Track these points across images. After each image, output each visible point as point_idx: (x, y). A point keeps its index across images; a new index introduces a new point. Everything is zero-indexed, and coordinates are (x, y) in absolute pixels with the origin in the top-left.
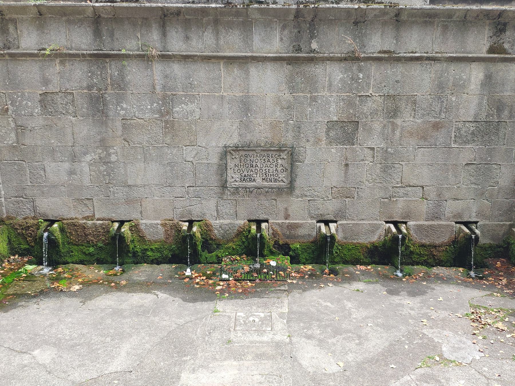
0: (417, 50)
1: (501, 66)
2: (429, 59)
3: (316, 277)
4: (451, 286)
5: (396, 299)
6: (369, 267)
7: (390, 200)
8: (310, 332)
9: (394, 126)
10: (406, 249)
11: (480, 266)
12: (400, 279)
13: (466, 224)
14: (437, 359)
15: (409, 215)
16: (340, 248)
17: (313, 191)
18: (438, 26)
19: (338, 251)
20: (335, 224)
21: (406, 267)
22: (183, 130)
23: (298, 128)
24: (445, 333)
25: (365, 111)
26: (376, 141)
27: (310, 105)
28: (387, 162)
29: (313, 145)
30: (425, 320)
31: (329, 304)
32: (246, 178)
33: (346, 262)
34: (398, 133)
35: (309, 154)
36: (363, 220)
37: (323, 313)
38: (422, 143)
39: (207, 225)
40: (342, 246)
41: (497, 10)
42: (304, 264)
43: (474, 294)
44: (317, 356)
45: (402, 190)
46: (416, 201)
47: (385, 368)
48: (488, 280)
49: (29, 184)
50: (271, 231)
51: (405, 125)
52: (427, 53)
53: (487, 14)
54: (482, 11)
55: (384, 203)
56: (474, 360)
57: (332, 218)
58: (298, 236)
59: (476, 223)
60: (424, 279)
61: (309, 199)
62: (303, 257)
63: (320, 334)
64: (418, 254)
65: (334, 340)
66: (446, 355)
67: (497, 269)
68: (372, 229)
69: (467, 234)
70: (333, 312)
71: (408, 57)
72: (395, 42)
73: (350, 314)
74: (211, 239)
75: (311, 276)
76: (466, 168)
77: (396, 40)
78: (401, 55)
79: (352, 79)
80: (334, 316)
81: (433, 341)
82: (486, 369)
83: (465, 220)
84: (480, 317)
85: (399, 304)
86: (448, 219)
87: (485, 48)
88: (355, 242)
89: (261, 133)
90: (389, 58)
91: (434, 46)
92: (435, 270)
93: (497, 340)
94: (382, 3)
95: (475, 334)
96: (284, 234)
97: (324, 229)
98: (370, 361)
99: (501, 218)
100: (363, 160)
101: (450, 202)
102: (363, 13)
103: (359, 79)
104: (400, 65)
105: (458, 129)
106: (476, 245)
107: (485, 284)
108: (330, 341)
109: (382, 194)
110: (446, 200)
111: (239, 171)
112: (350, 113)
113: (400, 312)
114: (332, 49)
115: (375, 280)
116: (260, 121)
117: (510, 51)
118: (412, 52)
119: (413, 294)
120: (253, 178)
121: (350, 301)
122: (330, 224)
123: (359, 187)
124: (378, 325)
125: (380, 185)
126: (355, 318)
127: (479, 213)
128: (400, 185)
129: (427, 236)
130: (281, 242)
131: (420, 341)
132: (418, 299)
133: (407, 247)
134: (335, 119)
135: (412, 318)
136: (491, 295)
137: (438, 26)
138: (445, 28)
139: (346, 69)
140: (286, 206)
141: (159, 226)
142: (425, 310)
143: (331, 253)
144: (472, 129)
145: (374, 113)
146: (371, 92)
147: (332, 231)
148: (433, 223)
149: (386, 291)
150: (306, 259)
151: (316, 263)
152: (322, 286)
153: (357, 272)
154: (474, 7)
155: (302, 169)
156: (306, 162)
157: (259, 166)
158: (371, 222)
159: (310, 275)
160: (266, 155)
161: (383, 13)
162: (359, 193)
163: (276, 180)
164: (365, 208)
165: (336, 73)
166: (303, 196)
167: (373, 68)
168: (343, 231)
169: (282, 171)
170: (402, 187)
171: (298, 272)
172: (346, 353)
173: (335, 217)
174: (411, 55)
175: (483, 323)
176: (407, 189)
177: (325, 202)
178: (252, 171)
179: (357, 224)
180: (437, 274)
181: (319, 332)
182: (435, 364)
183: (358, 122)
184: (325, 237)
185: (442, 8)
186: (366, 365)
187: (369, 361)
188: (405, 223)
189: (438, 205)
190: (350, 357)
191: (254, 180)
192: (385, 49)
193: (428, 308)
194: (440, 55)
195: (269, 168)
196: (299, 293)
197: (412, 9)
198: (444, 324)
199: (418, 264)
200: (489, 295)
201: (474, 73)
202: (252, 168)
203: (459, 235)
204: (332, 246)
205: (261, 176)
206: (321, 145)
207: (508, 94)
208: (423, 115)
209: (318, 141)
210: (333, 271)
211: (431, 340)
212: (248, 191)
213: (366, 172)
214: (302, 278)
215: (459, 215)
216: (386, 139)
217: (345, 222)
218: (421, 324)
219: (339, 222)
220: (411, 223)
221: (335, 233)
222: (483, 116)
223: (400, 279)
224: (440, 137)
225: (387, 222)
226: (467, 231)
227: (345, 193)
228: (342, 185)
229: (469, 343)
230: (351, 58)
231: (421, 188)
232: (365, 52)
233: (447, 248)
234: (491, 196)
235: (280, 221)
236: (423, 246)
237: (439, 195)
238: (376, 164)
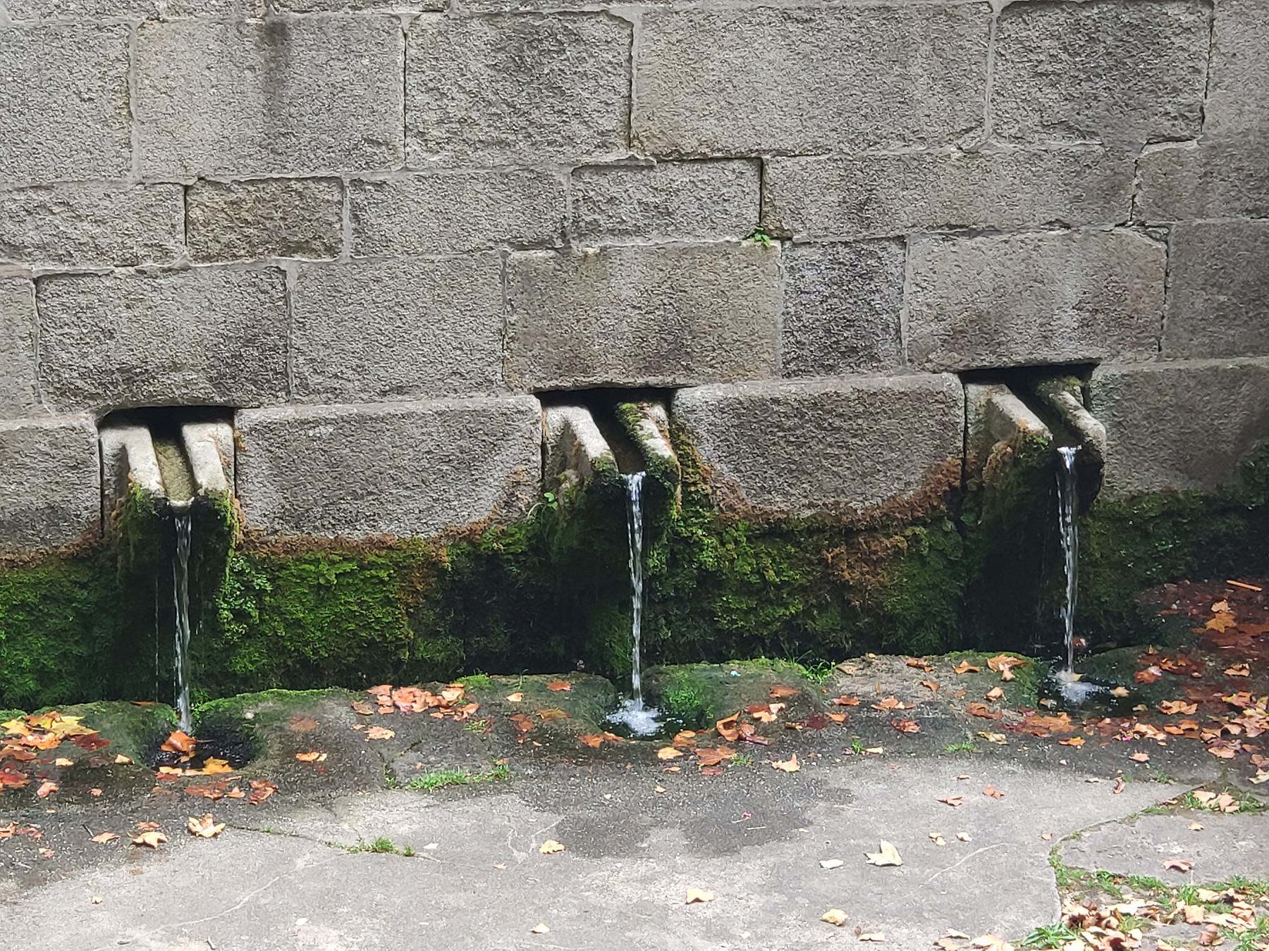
3: (106, 784)
5: (617, 880)
6: (451, 694)
7: (565, 252)
10: (673, 562)
11: (1115, 633)
13: (1027, 380)
15: (683, 340)
16: (261, 581)
17: (59, 220)
19: (250, 607)
20: (223, 431)
21: (681, 673)
33: (305, 674)
36: (400, 390)
40: (273, 569)
42: (30, 705)
45: (634, 188)
46: (724, 251)
48: (1160, 719)
55: (527, 275)
59: (1083, 369)
60: (784, 739)
61: (38, 269)
67: (1210, 643)
69: (1028, 442)
83: (1020, 355)
85: (642, 907)
86: (917, 359)
88: (357, 536)
92: (852, 679)
97: (148, 467)
101: (924, 248)
106: (1083, 509)
107: (1143, 742)
109: (511, 218)
110: (901, 240)
115: (487, 771)
119: (718, 838)
121: (333, 919)
123: (365, 175)
125: (495, 158)
127: (1102, 313)
129: (796, 471)
132: (752, 868)
133: (684, 548)
136: (1184, 804)
143: (204, 615)
147: (202, 479)
149: (561, 834)
150: (44, 676)
151: (111, 694)
152: (151, 838)
153: (376, 733)
158: (440, 404)
162: (369, 216)
164: (410, 315)
168: (279, 469)
170: (631, 166)
173: (216, 382)
177: (144, 284)
179: (362, 420)
180: (866, 705)
184: (158, 517)
188: (665, 396)
189: (857, 269)
193: (814, 915)
199: (747, 647)
203: (985, 451)
210: (223, 740)
215: (982, 328)
219: (249, 417)
220: (698, 396)
223: (641, 752)
225: (550, 398)
226: (1031, 422)
227: (275, 222)
228: (255, 166)
231: (750, 172)
233: (916, 539)
234: (1165, 198)
236: (775, 532)
237: (858, 210)
238: (463, 21)
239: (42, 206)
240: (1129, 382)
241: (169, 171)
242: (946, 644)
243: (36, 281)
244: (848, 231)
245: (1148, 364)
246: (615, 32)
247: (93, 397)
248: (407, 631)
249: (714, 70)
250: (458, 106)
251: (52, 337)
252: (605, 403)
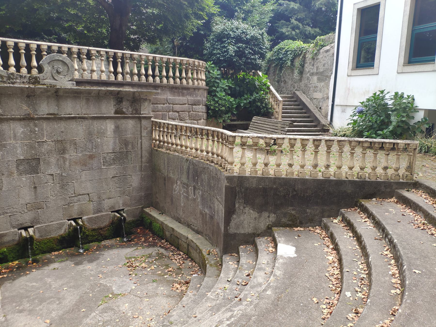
0: (72, 113)
1: (123, 121)
2: (80, 118)
4: (114, 250)
5: (81, 267)
6: (61, 252)
7: (69, 205)
8: (21, 308)
9: (65, 160)
10: (83, 234)
11: (129, 234)
12: (82, 254)
13: (118, 211)
14: (111, 296)
15: (82, 213)
16: (38, 244)
18: (83, 99)
19: (37, 246)
20: (33, 229)
21: (85, 245)
24: (114, 279)
25: (43, 151)
26: (54, 170)
28: (63, 182)
29: (8, 177)
30: (100, 275)
31: (34, 284)
33: (44, 252)
34: (67, 163)
37: (30, 291)
38: (84, 168)
40: (39, 242)
41: (116, 90)
42: (12, 261)
43: (127, 251)
44: (29, 322)
45: (76, 198)
47: (78, 313)
48: (134, 241)
51: (71, 158)
52: (79, 114)
53: (111, 92)
54: (108, 91)
55: (65, 208)
56: (132, 289)
57: (30, 225)
58: (5, 243)
59: (123, 210)
60: (97, 250)
61: (10, 215)
62: (10, 257)
63: (29, 306)
65: (41, 307)
66: (115, 292)
67: (138, 233)
69: (118, 217)
70: (38, 288)
71: (67, 117)
72: (57, 108)
73: (51, 286)
75: (18, 268)
76: (113, 179)
77: (58, 107)
78: (62, 116)
79: (31, 131)
80: (39, 291)
81: (107, 286)
82: (139, 293)
83: (117, 209)
84: (132, 264)
85: (83, 270)
86: (107, 211)
87: (113, 112)
90: (54, 118)
91: (83, 110)
92: (103, 243)
93: (143, 274)
94: (45, 84)
95: (130, 274)
97: (24, 233)
98: (68, 312)
99: (137, 204)
100: (46, 183)
101: (106, 201)
102: (33, 90)
103: (36, 131)
104: (63, 122)
105: (105, 157)
106: (124, 223)
107: (133, 244)
108: (38, 309)
109: (63, 203)
112: (32, 153)
113: (84, 275)
114: (13, 113)
115: (65, 259)
117: (127, 113)
118: (69, 114)
119: (91, 261)
121: (50, 277)
122: (29, 230)
124: (70, 287)
126: (54, 288)
127: (124, 204)
128: (74, 195)
131: (99, 289)
132: (95, 263)
133: (84, 233)
134: (22, 158)
135: (92, 276)
136: (137, 249)
137: (83, 99)
138: (88, 100)
139: (25, 125)
142: (100, 269)
144: (112, 157)
145: (49, 152)
146: (45, 139)
147: (30, 234)
148: (98, 215)
149: (74, 264)
150: (13, 258)
151: (22, 258)
152: (28, 273)
153: (53, 257)
154: (103, 88)
156: (4, 189)
159: (17, 268)
161: (46, 90)
162: (47, 204)
164: (53, 214)
165: (19, 129)
167: (44, 124)
168: (39, 231)
171: (7, 268)
172: (51, 313)
174: (69, 116)
175: (134, 266)
176: (78, 197)
177: (22, 215)
180: (105, 245)
181: (28, 305)
182: (110, 300)
183: (39, 159)
184: (26, 239)
185: (84, 88)
186: (66, 316)
187: (67, 313)
188: (81, 218)
189: (100, 203)
190: (54, 314)
192: (51, 112)
193: (102, 267)
194: (87, 116)
196: (9, 283)
197: (65, 88)
198: (112, 273)
199: (92, 242)
200: (135, 250)
201: (109, 125)
203: (114, 219)
204: (32, 245)
206: (14, 177)
207: (129, 136)
208: (82, 151)
209: (11, 174)
210: (34, 261)
211: (105, 286)
213: (50, 190)
214: (11, 271)
215: (113, 207)
216: (60, 167)
217: (40, 226)
218: (98, 278)
220: (84, 218)
221: (33, 234)
222: (117, 149)
223: (82, 254)
224: (95, 163)
225: (69, 220)
226: (119, 215)
227: (36, 206)
229: (128, 280)
230: (27, 118)
231: (88, 195)
232: (37, 115)
236: (94, 230)
237: (99, 198)
240: (128, 210)
242: (112, 238)
244: (98, 200)
245: (129, 208)
246: (73, 184)
248: (55, 246)
249: (83, 186)
250: (56, 192)
251: (12, 221)
252: (75, 220)
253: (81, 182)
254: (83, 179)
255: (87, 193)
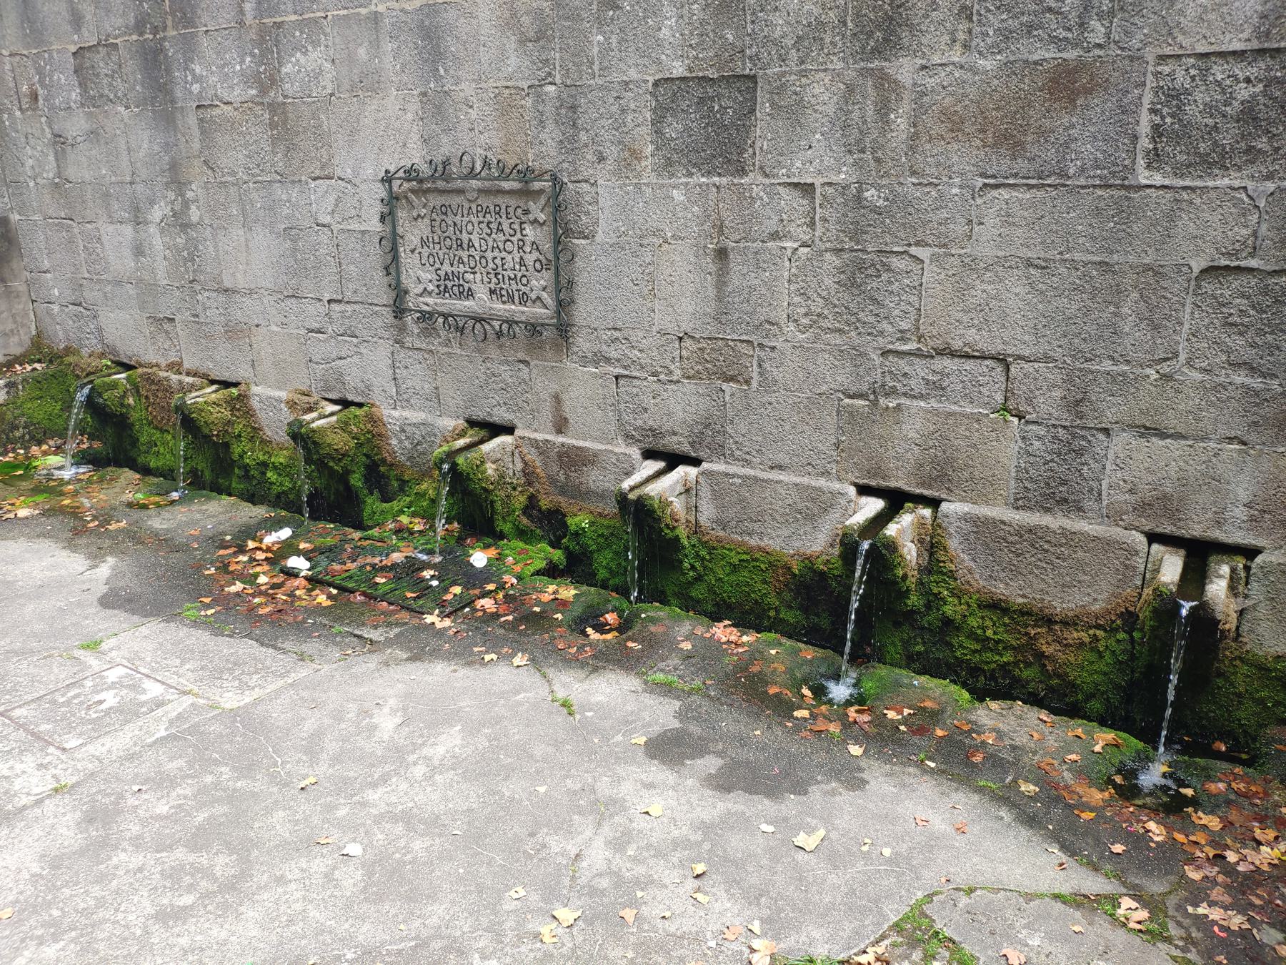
7: (875, 403)
9: (886, 87)
16: (703, 553)
19: (697, 565)
22: (306, 130)
23: (570, 110)
25: (778, 33)
26: (820, 159)
27: (600, 22)
29: (617, 173)
32: (449, 284)
34: (900, 122)
35: (607, 204)
36: (780, 467)
38: (1000, 164)
39: (374, 420)
40: (711, 550)
45: (920, 369)
46: (978, 419)
49: (87, 275)
50: (519, 465)
51: (930, 82)
55: (853, 414)
57: (685, 448)
64: (972, 635)
68: (805, 506)
74: (384, 461)
83: (1195, 530)
86: (1113, 516)
88: (753, 542)
89: (479, 136)
96: (552, 480)
100: (775, 236)
101: (1121, 442)
109: (843, 378)
110: (1106, 431)
111: (431, 260)
116: (468, 88)
120: (466, 286)
123: (765, 341)
125: (836, 339)
129: (1015, 571)
130: (544, 503)
134: (679, 70)
140: (555, 387)
141: (283, 405)
144: (1243, 92)
155: (591, 262)
156: (600, 237)
157: (477, 245)
160: (492, 208)
162: (767, 365)
163: (524, 299)
166: (599, 359)
168: (716, 496)
169: (538, 266)
170: (917, 354)
173: (692, 444)
178: (461, 261)
179: (756, 479)
183: (753, 78)
191: (470, 294)
195: (504, 254)
202: (460, 253)
205: (486, 279)
212: (460, 326)
213: (789, 280)
215: (1164, 504)
219: (705, 465)
224: (1083, 135)
227: (721, 364)
228: (711, 330)
231: (999, 369)
233: (1095, 638)
235: (540, 436)
236: (996, 606)
237: (1076, 405)
238: (821, 253)
239: (617, 339)
241: (671, 328)
243: (617, 378)
246: (916, 268)
247: (639, 441)
248: (773, 600)
249: (976, 296)
250: (817, 305)
251: (622, 406)
253: (971, 264)
254: (986, 245)
255: (999, 347)
